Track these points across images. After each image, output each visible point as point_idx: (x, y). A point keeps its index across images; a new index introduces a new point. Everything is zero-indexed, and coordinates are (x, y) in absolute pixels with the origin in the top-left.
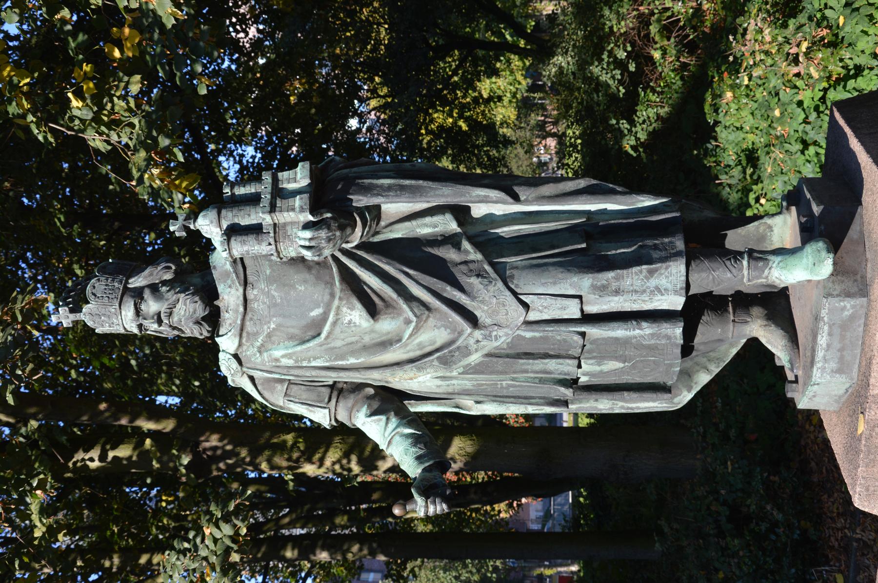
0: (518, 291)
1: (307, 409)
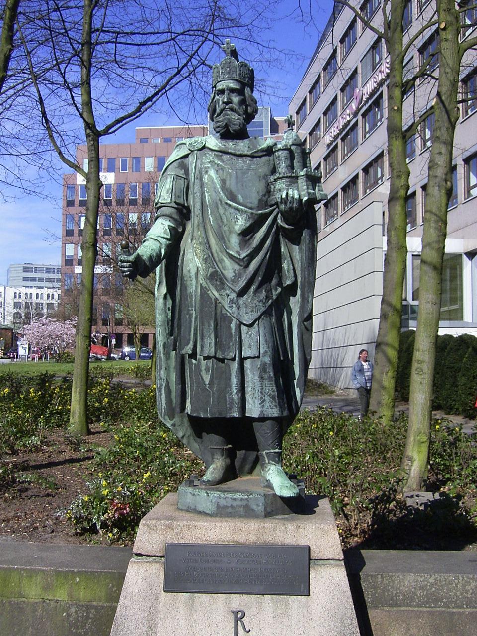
0: (261, 320)
1: (170, 189)
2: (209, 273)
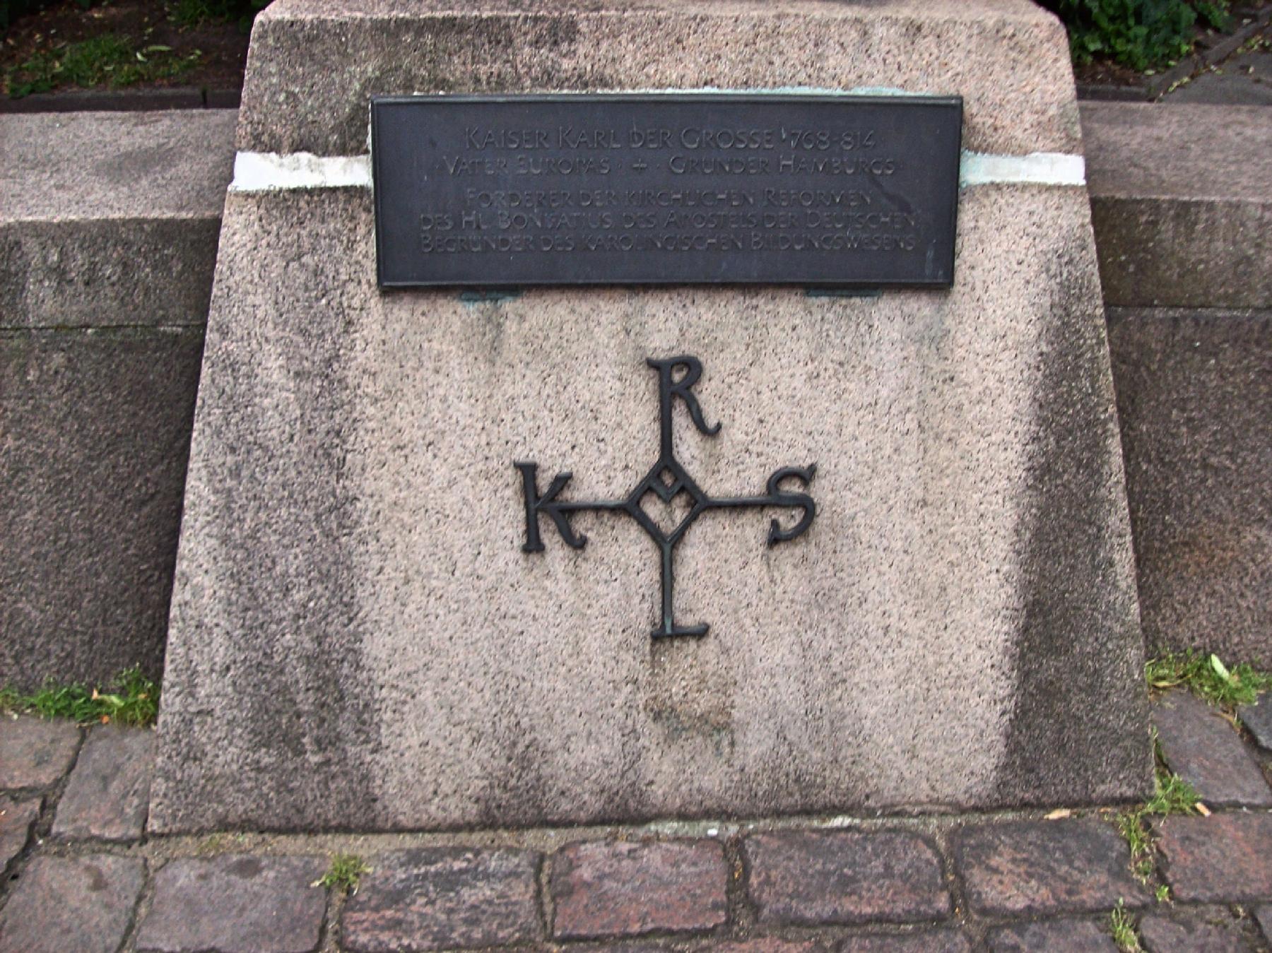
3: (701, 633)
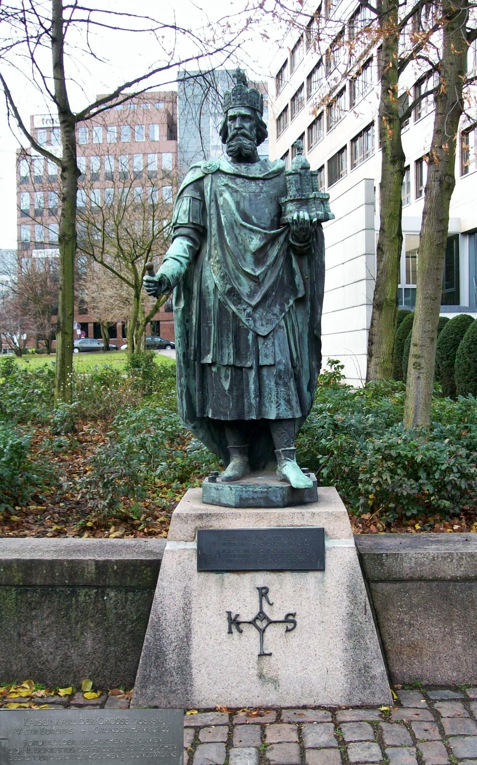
2: (227, 289)
3: (270, 654)
